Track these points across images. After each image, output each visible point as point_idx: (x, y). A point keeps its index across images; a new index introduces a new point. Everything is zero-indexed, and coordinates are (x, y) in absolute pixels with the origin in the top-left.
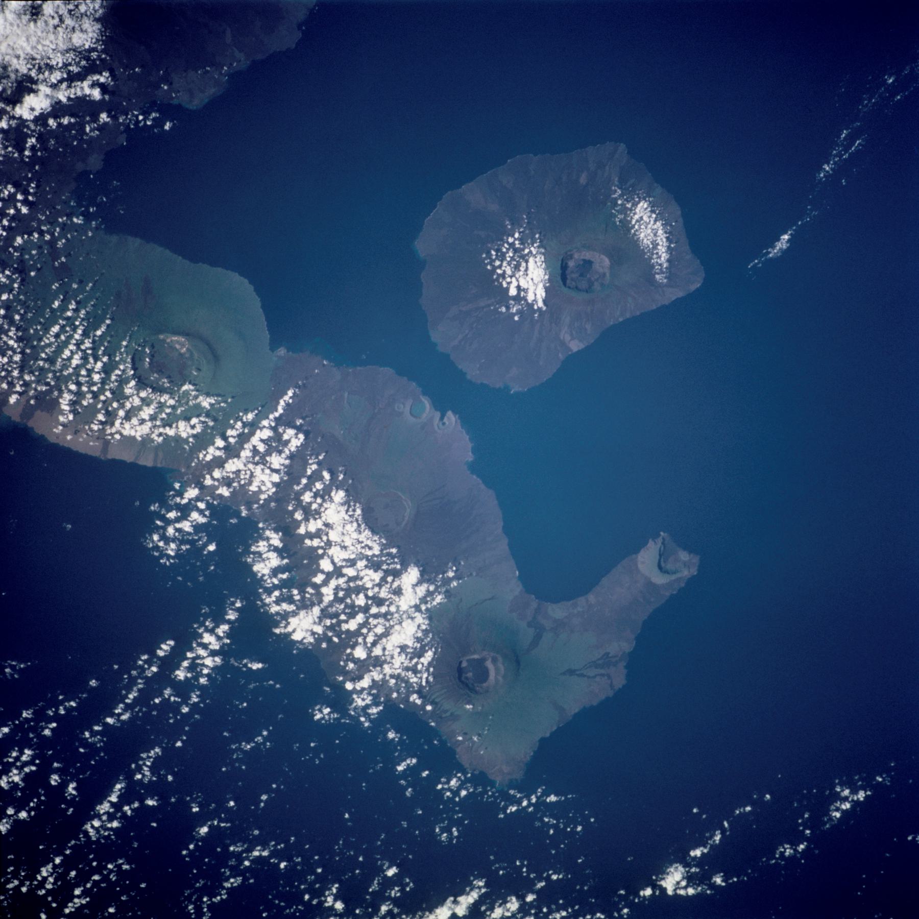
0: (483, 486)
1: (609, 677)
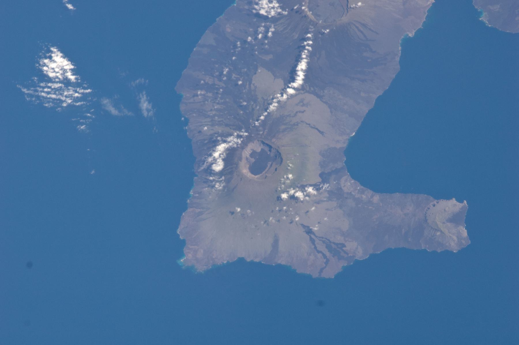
0: (398, 59)
1: (327, 263)
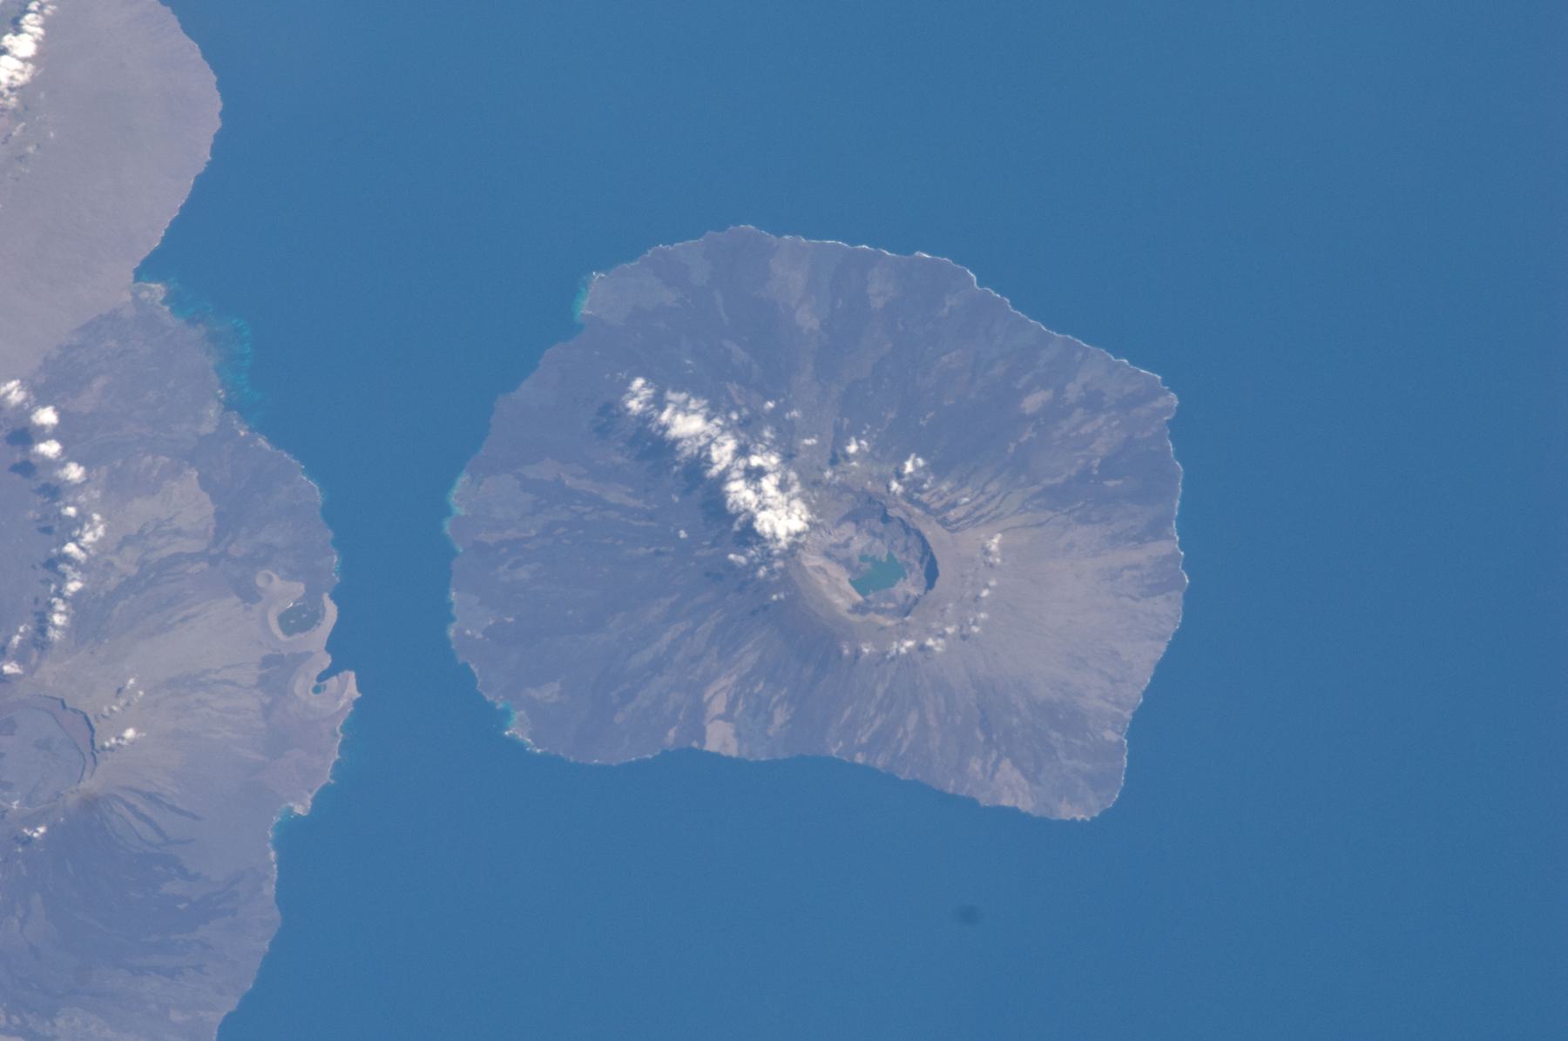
0: (270, 890)
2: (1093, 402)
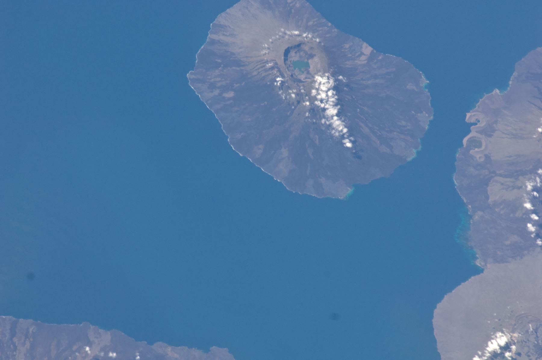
2: (212, 86)
